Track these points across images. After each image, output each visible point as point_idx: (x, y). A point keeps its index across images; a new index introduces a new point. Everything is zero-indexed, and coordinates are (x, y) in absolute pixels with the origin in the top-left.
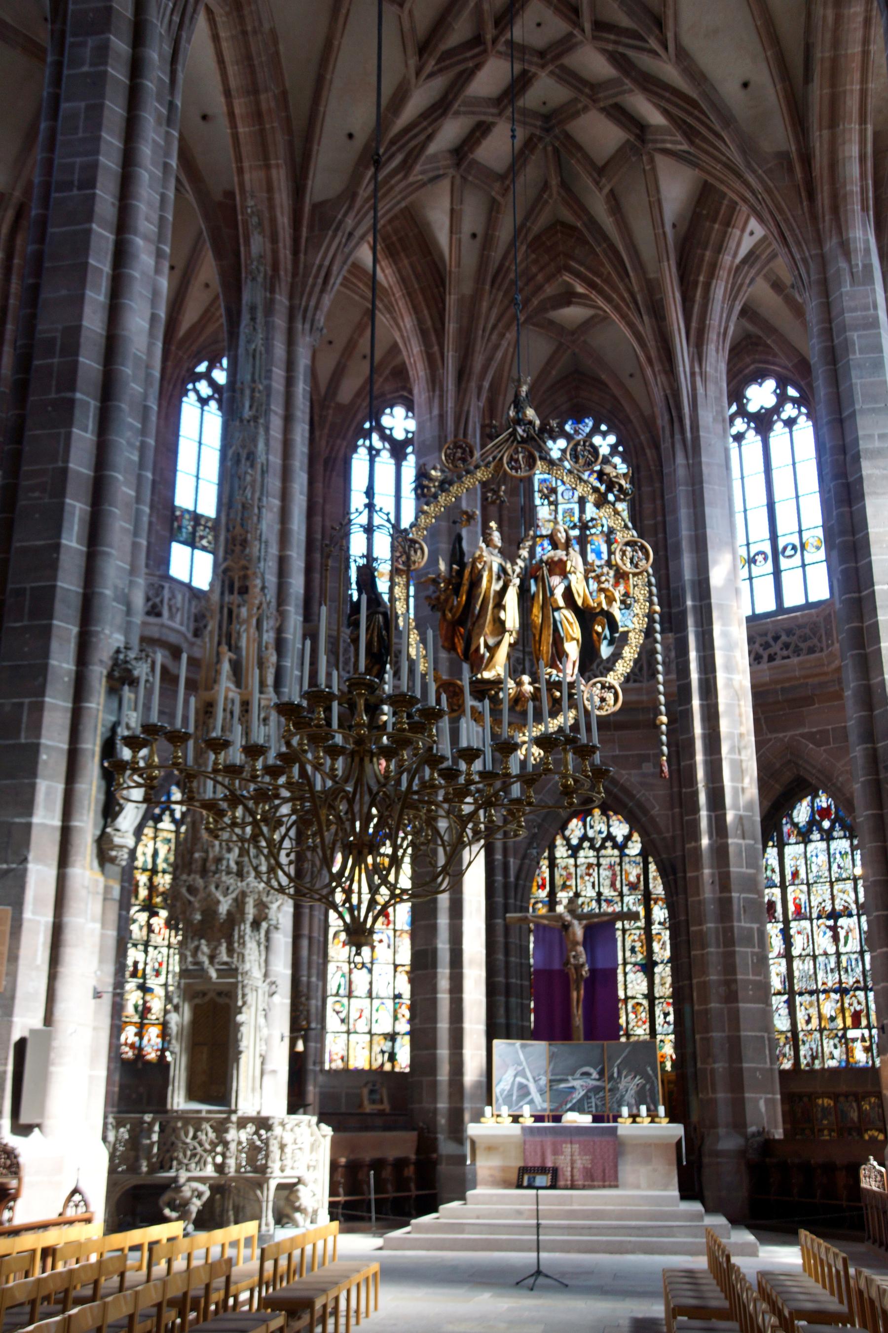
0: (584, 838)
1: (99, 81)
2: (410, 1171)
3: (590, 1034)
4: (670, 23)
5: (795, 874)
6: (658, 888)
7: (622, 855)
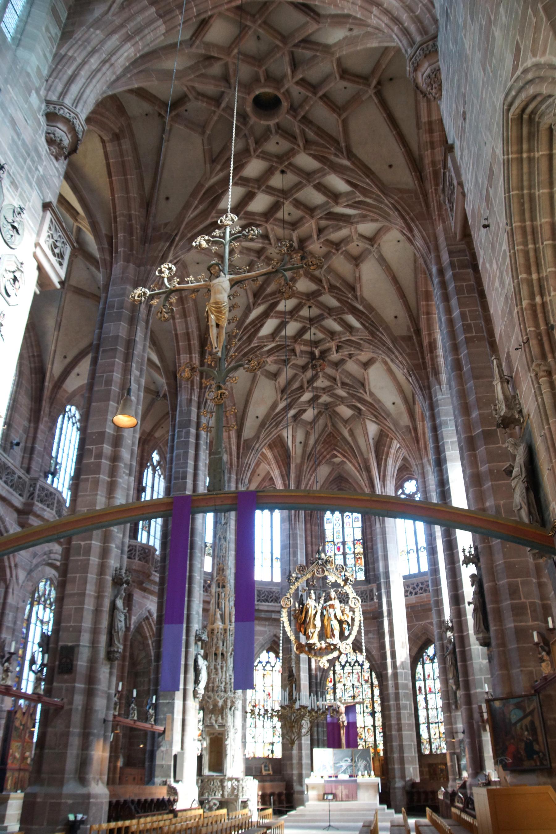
0: (347, 662)
1: (187, 443)
2: (283, 797)
3: (348, 746)
4: (367, 384)
5: (429, 676)
6: (376, 682)
7: (362, 669)
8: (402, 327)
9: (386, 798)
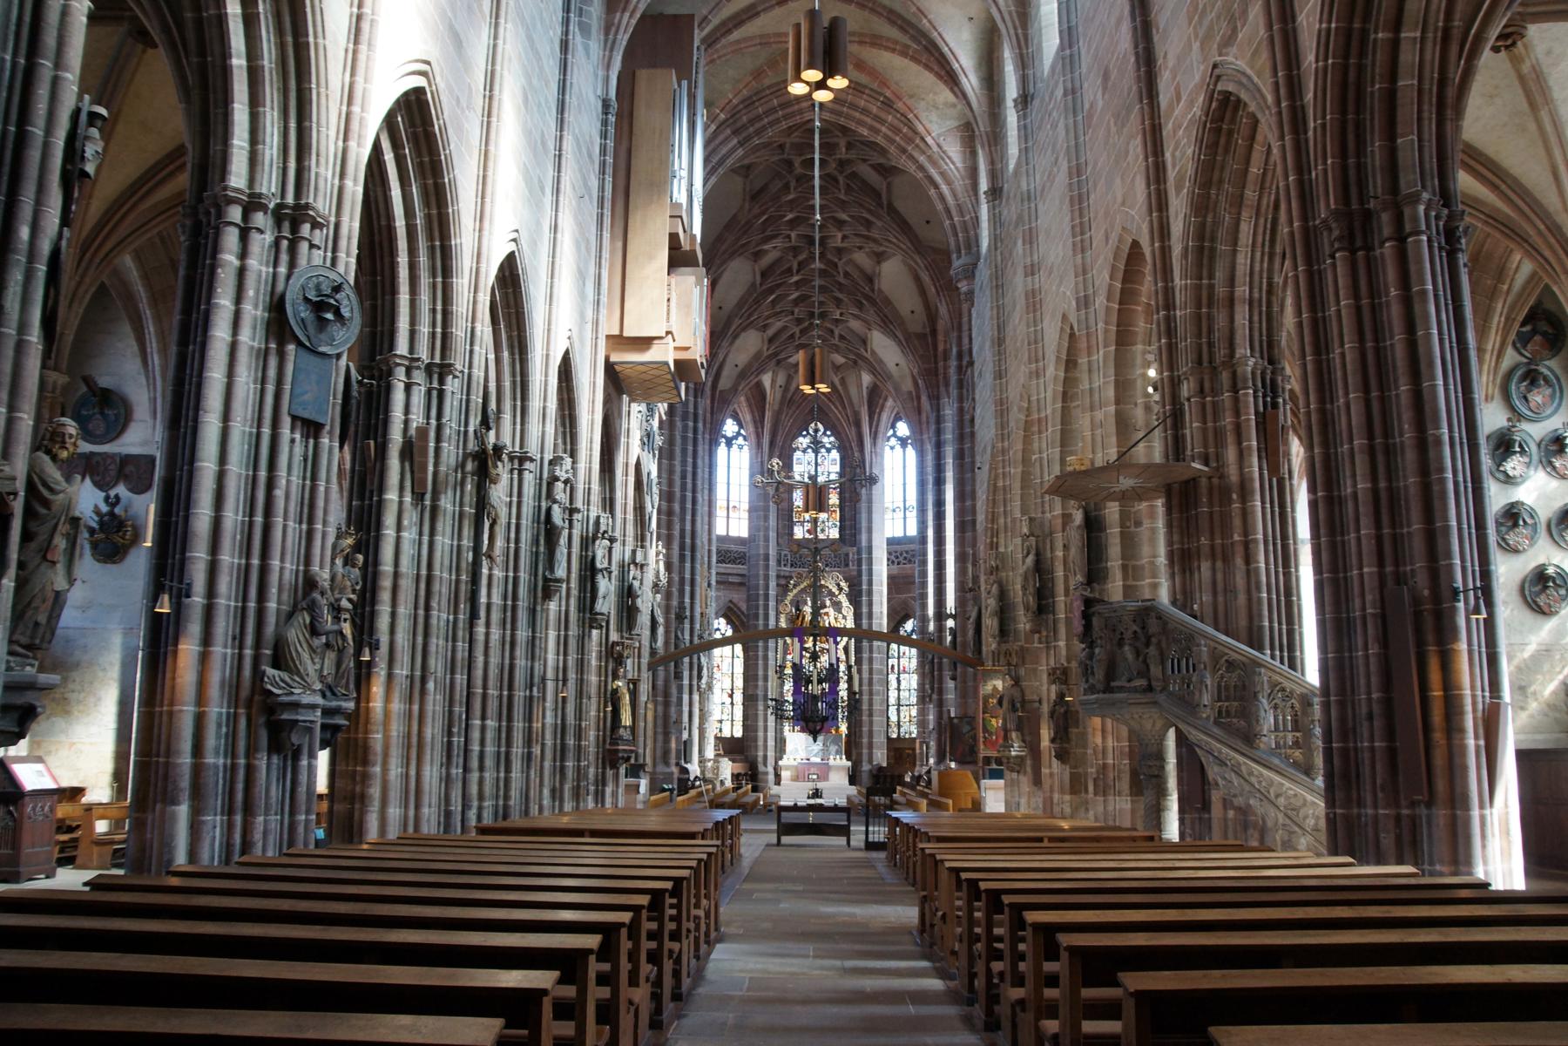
8: (917, 324)
9: (853, 780)
